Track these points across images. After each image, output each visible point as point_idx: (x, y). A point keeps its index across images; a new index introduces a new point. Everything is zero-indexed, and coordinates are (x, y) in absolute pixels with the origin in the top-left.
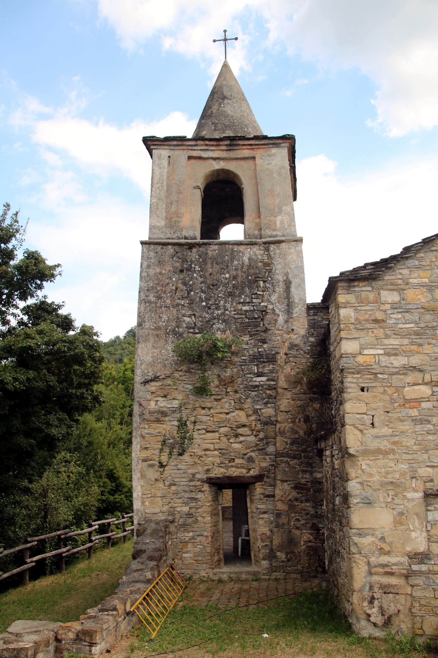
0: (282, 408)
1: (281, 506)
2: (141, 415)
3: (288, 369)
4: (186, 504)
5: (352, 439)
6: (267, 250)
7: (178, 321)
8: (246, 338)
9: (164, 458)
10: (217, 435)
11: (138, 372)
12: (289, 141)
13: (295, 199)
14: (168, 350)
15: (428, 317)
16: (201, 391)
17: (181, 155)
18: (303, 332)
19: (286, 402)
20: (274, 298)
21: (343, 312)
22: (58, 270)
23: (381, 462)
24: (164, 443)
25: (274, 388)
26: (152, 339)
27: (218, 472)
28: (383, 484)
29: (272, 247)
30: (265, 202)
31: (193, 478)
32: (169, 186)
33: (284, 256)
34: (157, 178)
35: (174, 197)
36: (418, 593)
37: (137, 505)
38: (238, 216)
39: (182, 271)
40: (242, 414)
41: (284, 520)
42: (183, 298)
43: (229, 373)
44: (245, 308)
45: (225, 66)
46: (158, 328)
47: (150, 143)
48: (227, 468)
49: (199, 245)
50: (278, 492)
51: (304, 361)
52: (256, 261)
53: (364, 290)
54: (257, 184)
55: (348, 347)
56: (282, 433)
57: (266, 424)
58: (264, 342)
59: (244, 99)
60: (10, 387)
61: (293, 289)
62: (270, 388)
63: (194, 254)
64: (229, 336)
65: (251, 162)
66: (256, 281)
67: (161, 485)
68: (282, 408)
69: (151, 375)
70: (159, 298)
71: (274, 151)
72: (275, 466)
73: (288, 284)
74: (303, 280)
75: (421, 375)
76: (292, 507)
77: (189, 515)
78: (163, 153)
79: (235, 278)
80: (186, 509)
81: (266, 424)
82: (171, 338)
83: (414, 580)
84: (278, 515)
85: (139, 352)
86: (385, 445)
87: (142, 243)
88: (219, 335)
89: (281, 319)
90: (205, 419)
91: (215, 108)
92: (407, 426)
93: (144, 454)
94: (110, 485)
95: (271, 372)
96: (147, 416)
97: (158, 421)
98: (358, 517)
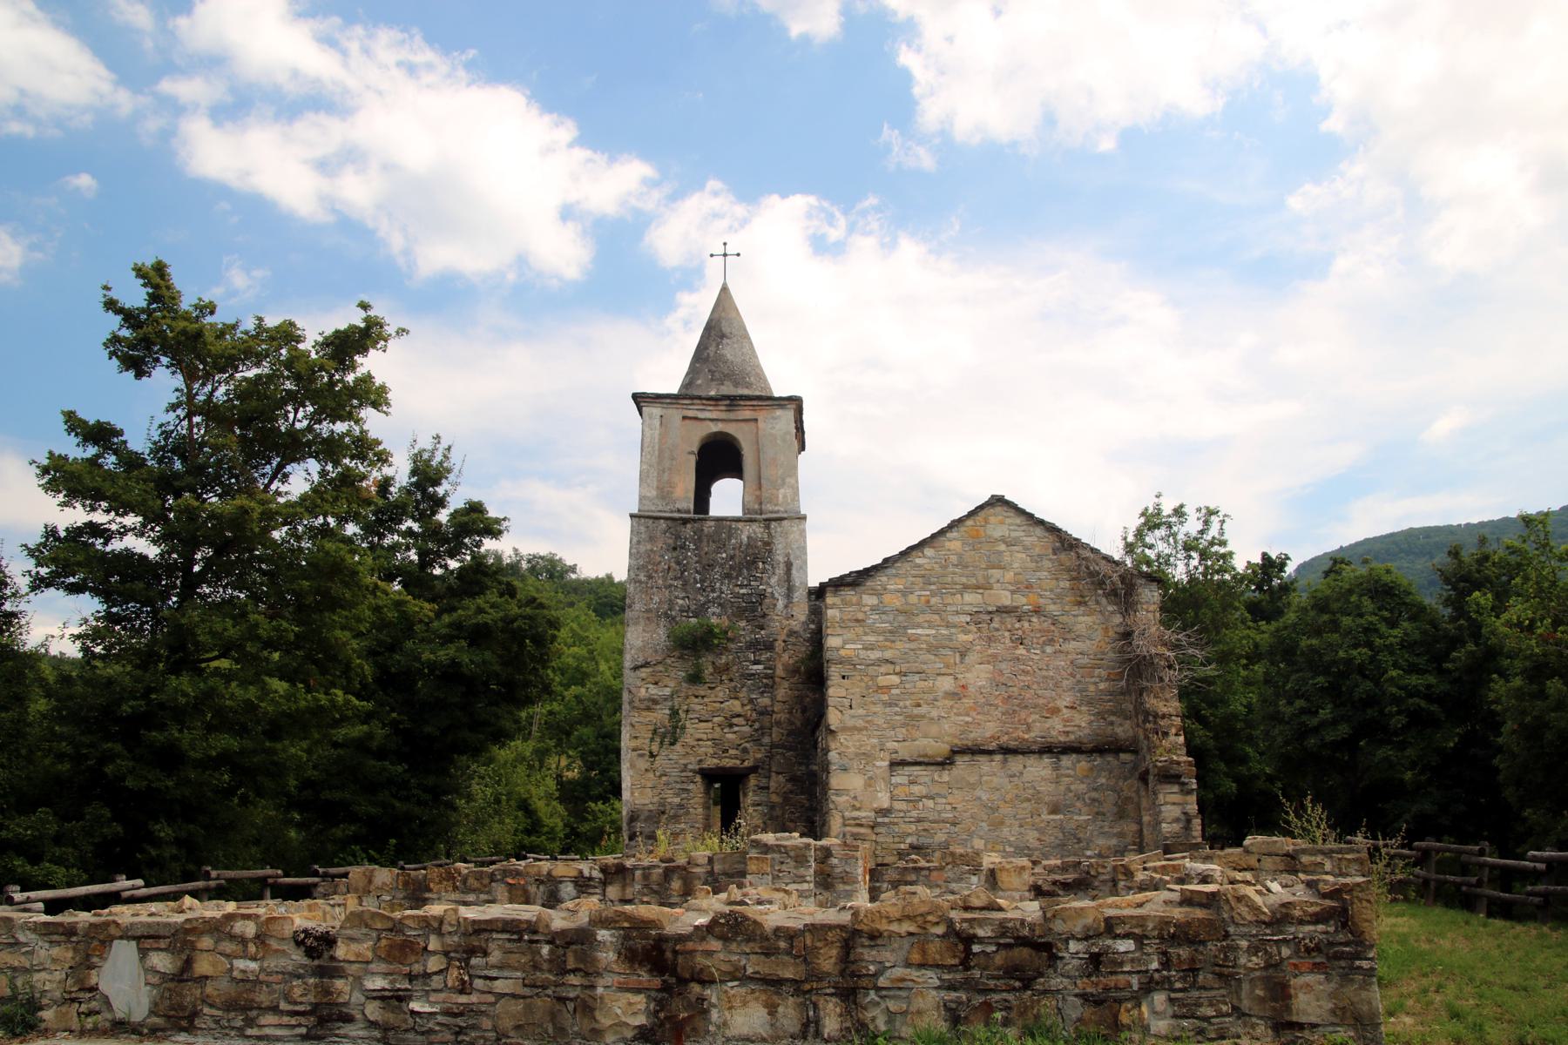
0: (779, 698)
1: (775, 798)
2: (631, 702)
3: (786, 656)
4: (678, 795)
5: (833, 718)
6: (768, 527)
7: (671, 604)
8: (743, 624)
9: (655, 748)
10: (710, 725)
11: (628, 657)
12: (796, 403)
13: (802, 448)
14: (661, 634)
15: (901, 618)
16: (695, 678)
17: (675, 414)
18: (803, 618)
19: (782, 692)
20: (773, 581)
21: (830, 612)
22: (505, 524)
23: (857, 737)
24: (655, 732)
25: (771, 677)
26: (642, 622)
27: (711, 763)
28: (857, 755)
29: (773, 524)
30: (765, 473)
31: (685, 768)
32: (661, 451)
33: (786, 534)
34: (647, 440)
35: (667, 464)
36: (880, 839)
37: (626, 795)
38: (736, 470)
39: (675, 549)
40: (737, 703)
41: (778, 812)
42: (676, 579)
43: (724, 660)
44: (743, 591)
45: (724, 289)
46: (648, 611)
47: (640, 399)
48: (720, 758)
49: (694, 520)
50: (773, 784)
51: (803, 649)
52: (756, 540)
53: (849, 594)
54: (758, 451)
55: (832, 642)
56: (778, 723)
57: (761, 714)
58: (762, 628)
59: (746, 336)
60: (465, 670)
61: (794, 572)
62: (767, 676)
63: (688, 530)
64: (725, 622)
65: (752, 425)
66: (754, 562)
67: (651, 775)
68: (779, 698)
69: (641, 661)
70: (650, 577)
71: (779, 412)
72: (771, 757)
73: (789, 565)
74: (805, 562)
75: (891, 667)
76: (786, 799)
77: (681, 806)
78: (654, 411)
79: (732, 558)
80: (677, 800)
81: (761, 714)
82: (663, 622)
83: (878, 830)
84: (772, 807)
85: (629, 635)
86: (860, 723)
87: (632, 516)
88: (714, 620)
89: (781, 604)
90: (698, 707)
91: (712, 349)
92: (878, 708)
93: (634, 744)
94: (524, 822)
95: (769, 660)
96: (637, 704)
97: (648, 709)
98: (836, 781)
